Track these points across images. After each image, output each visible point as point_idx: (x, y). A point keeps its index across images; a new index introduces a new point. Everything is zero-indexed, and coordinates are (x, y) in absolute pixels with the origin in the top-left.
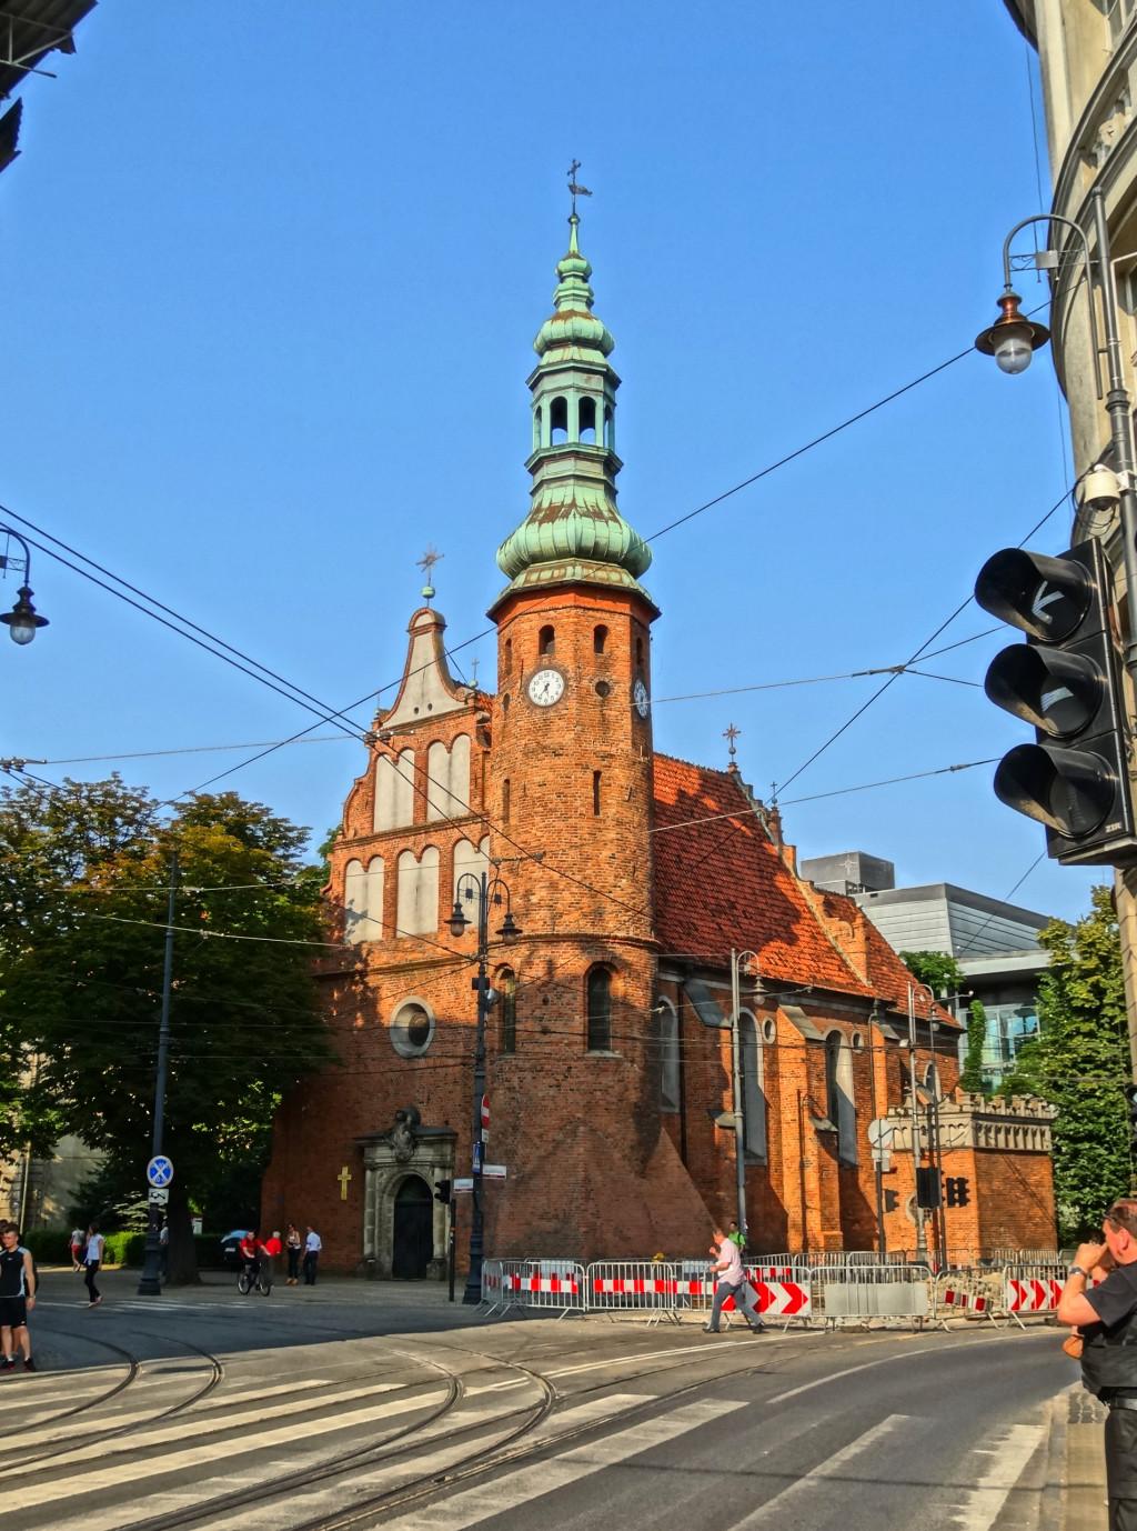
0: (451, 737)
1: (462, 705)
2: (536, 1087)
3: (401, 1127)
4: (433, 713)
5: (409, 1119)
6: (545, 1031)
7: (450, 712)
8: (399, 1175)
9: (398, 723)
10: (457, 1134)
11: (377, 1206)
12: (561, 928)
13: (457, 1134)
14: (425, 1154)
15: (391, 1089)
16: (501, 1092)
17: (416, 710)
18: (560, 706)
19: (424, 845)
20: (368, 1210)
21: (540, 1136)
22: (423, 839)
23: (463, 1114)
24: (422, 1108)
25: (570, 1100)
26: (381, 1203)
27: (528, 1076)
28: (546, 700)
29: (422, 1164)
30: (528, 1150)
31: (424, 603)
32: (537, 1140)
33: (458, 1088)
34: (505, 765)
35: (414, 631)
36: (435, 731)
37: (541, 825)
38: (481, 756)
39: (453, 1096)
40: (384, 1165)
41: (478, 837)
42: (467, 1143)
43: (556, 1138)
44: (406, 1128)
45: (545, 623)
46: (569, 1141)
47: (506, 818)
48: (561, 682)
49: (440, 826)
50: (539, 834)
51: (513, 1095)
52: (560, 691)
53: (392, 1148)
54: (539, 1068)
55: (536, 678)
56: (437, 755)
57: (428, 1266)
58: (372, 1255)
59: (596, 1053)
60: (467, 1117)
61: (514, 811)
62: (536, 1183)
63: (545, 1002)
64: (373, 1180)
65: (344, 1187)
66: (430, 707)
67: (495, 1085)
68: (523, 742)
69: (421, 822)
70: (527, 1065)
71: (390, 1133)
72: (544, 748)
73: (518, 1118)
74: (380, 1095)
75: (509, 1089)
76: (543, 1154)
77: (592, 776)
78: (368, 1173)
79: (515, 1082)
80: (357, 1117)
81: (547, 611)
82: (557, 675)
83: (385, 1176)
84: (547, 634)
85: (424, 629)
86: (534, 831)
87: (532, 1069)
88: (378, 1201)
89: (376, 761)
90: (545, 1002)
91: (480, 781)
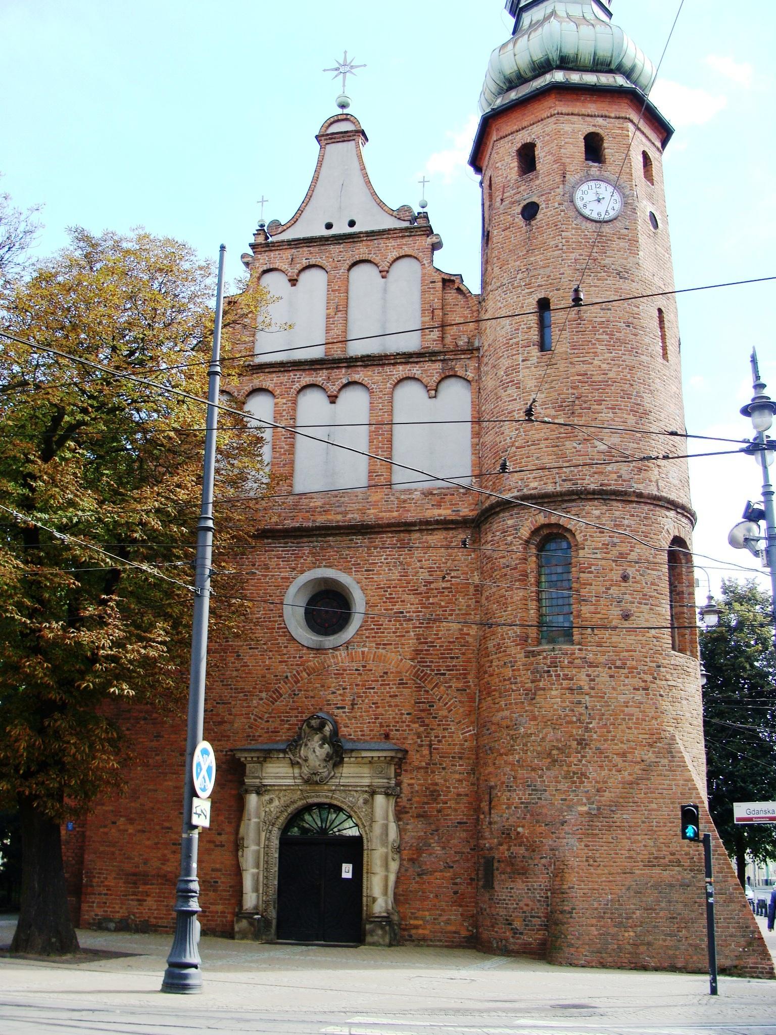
0: (390, 258)
2: (614, 688)
5: (328, 729)
7: (389, 230)
8: (300, 803)
9: (301, 236)
10: (406, 752)
12: (640, 486)
13: (407, 751)
14: (354, 774)
15: (284, 689)
16: (554, 693)
17: (329, 226)
18: (618, 224)
19: (345, 381)
21: (623, 755)
22: (343, 375)
23: (417, 725)
27: (603, 675)
29: (347, 789)
30: (605, 773)
31: (340, 111)
32: (617, 760)
33: (406, 692)
34: (540, 281)
35: (326, 138)
36: (362, 250)
39: (398, 700)
40: (281, 789)
41: (436, 378)
42: (424, 764)
43: (645, 757)
44: (324, 740)
45: (592, 129)
46: (665, 761)
51: (578, 698)
52: (618, 206)
53: (293, 764)
54: (618, 663)
55: (584, 187)
59: (673, 652)
62: (624, 816)
63: (625, 578)
64: (258, 808)
66: (352, 224)
67: (541, 684)
68: (573, 256)
69: (337, 353)
70: (602, 659)
71: (295, 744)
73: (587, 729)
74: (264, 695)
75: (571, 689)
76: (628, 778)
80: (222, 723)
81: (595, 116)
83: (276, 803)
84: (594, 148)
85: (345, 137)
86: (595, 362)
87: (610, 664)
89: (259, 278)
90: (625, 578)
91: (439, 313)
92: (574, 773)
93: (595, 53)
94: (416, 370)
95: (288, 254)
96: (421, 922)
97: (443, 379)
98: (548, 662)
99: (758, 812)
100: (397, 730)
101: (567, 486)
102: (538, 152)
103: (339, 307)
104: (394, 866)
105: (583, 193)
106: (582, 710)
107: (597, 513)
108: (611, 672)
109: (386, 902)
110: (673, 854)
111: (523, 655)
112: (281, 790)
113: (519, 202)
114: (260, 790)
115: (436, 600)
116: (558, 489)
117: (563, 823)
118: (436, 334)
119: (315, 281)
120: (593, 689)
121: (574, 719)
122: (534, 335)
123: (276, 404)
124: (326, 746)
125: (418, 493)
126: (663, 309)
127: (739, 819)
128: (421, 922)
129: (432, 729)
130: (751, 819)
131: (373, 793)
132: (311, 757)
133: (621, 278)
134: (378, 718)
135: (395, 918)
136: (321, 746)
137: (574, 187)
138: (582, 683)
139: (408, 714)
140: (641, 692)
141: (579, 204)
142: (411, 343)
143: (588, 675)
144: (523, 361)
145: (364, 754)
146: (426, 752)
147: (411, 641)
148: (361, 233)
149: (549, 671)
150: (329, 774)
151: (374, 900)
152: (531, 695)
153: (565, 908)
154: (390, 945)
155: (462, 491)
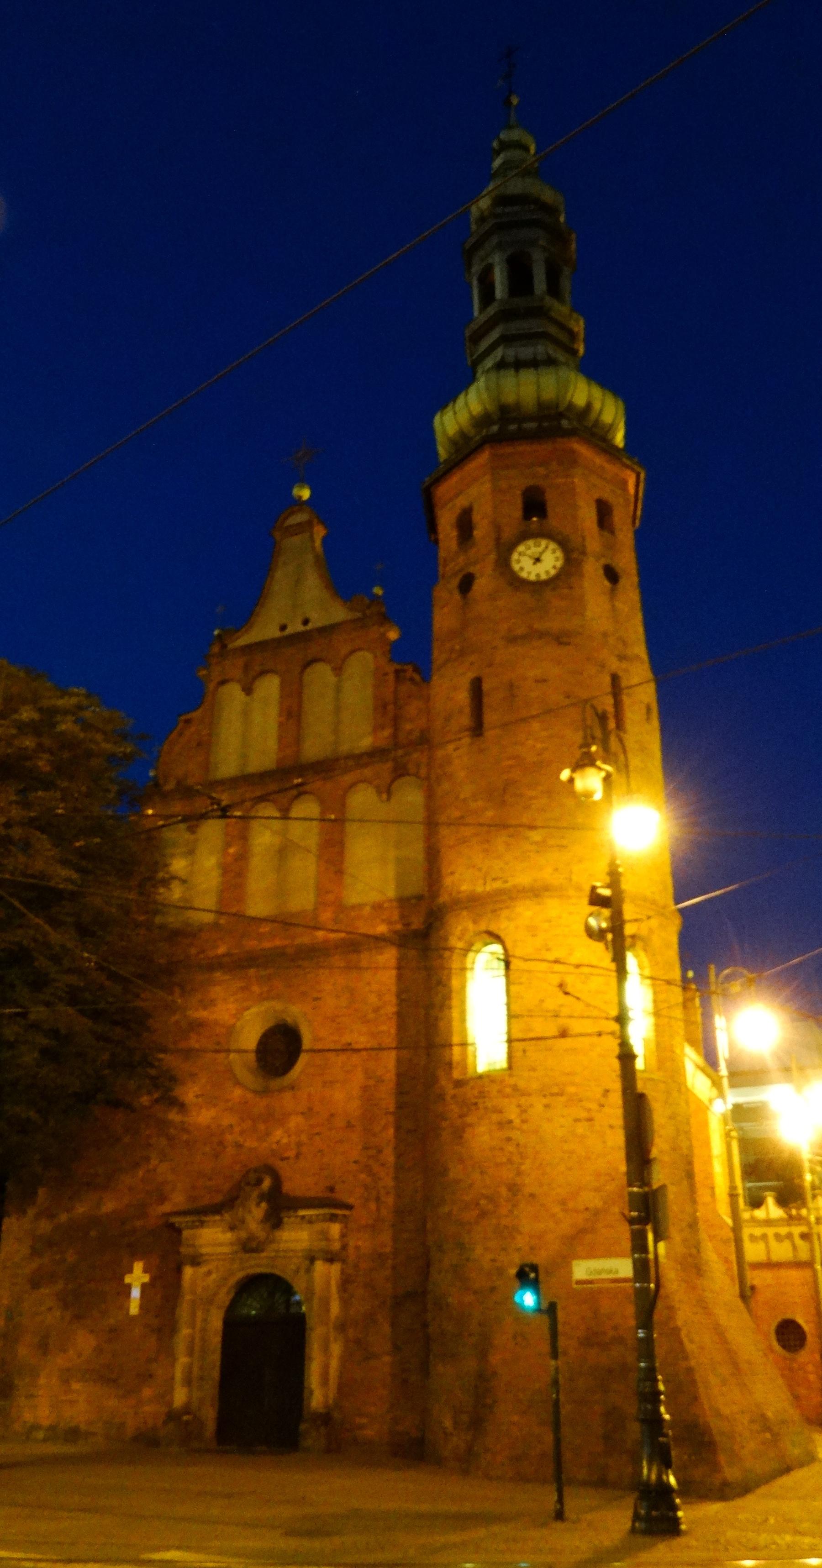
1: (359, 615)
2: (549, 1120)
3: (255, 1194)
4: (310, 626)
5: (267, 1183)
6: (564, 1034)
8: (240, 1275)
11: (199, 1325)
13: (350, 1207)
16: (482, 1129)
17: (283, 628)
20: (185, 1332)
21: (563, 1203)
23: (363, 1176)
24: (285, 1169)
25: (610, 1144)
26: (205, 1320)
28: (538, 575)
32: (557, 1209)
37: (544, 734)
38: (391, 677)
42: (370, 1222)
43: (591, 1206)
44: (262, 1197)
45: (531, 482)
47: (477, 728)
48: (559, 554)
49: (325, 768)
50: (539, 746)
52: (559, 564)
53: (232, 1228)
54: (555, 1090)
55: (521, 548)
56: (321, 675)
57: (303, 1427)
58: (187, 1409)
60: (369, 1179)
61: (490, 717)
65: (136, 1293)
66: (306, 622)
67: (469, 1120)
70: (535, 1086)
72: (542, 635)
73: (519, 1173)
74: (207, 1149)
77: (607, 680)
78: (188, 1272)
79: (512, 1113)
82: (553, 546)
83: (214, 1276)
87: (544, 1092)
88: (199, 1314)
91: (391, 707)
92: (506, 1227)
93: (539, 398)
94: (367, 772)
95: (241, 662)
96: (364, 1421)
97: (393, 781)
98: (476, 1092)
99: (600, 1272)
100: (343, 1182)
101: (498, 885)
102: (476, 517)
103: (293, 714)
104: (336, 1349)
105: (520, 554)
106: (511, 1148)
107: (528, 914)
108: (545, 1101)
109: (326, 1396)
110: (615, 1328)
111: (451, 1086)
112: (219, 1260)
113: (455, 574)
114: (196, 1261)
115: (384, 1028)
116: (488, 888)
117: (493, 1289)
118: (387, 733)
119: (270, 687)
120: (524, 1121)
121: (504, 1160)
122: (466, 720)
123: (227, 825)
124: (264, 1205)
125: (368, 909)
126: (621, 674)
127: (579, 1282)
128: (364, 1421)
129: (380, 1179)
130: (591, 1282)
131: (312, 1260)
132: (249, 1218)
133: (560, 643)
134: (321, 1169)
135: (336, 1415)
136: (258, 1205)
137: (512, 547)
138: (513, 1117)
139: (356, 1162)
140: (586, 1123)
141: (516, 567)
142: (366, 743)
143: (519, 1106)
144: (455, 750)
145: (302, 1213)
146: (373, 1206)
147: (359, 1077)
148: (311, 631)
149: (476, 1104)
150: (267, 1238)
151: (311, 1393)
152: (459, 1133)
153: (489, 1401)
154: (328, 1451)
155: (413, 901)
